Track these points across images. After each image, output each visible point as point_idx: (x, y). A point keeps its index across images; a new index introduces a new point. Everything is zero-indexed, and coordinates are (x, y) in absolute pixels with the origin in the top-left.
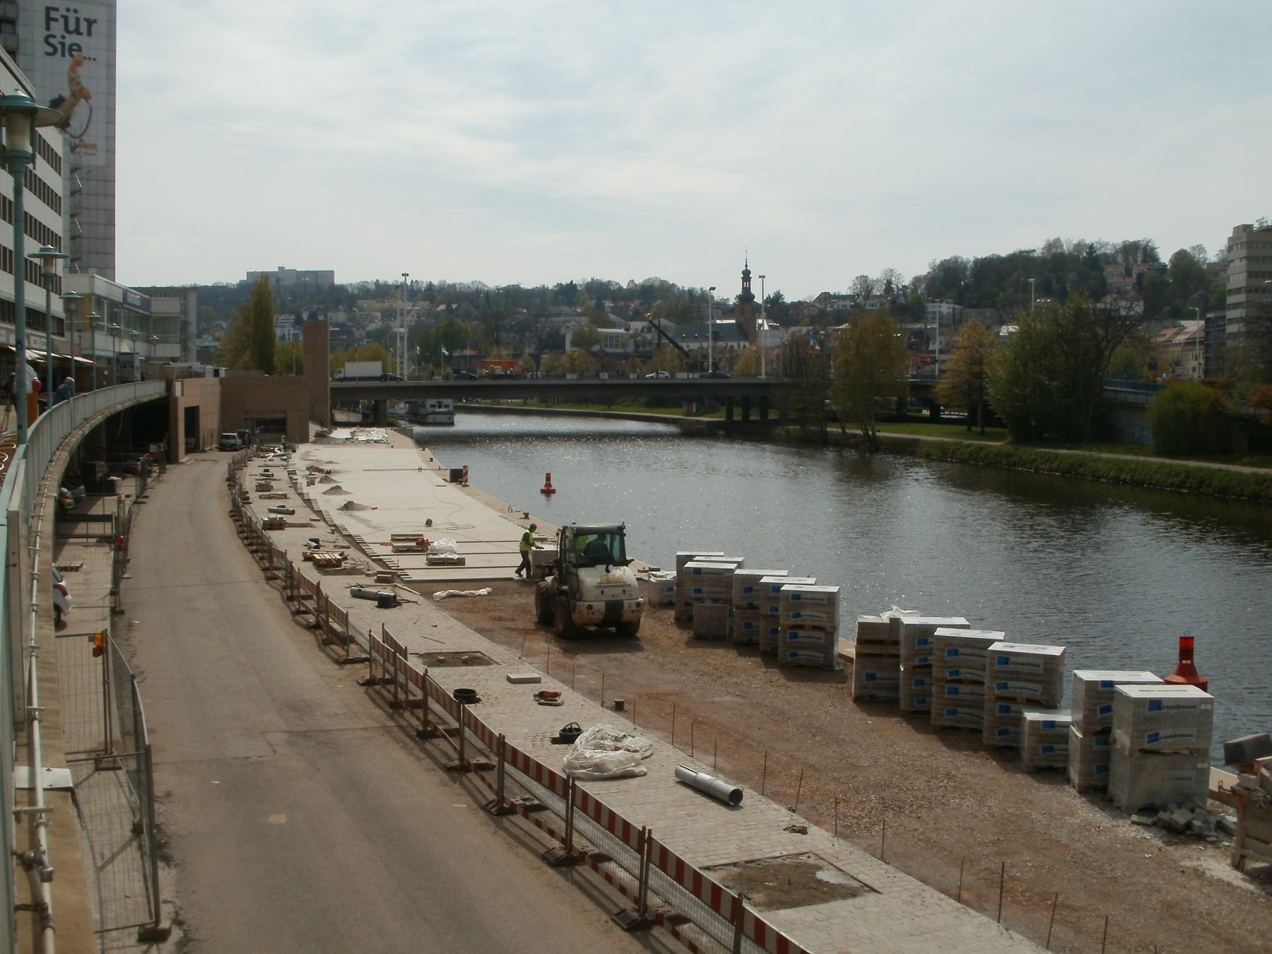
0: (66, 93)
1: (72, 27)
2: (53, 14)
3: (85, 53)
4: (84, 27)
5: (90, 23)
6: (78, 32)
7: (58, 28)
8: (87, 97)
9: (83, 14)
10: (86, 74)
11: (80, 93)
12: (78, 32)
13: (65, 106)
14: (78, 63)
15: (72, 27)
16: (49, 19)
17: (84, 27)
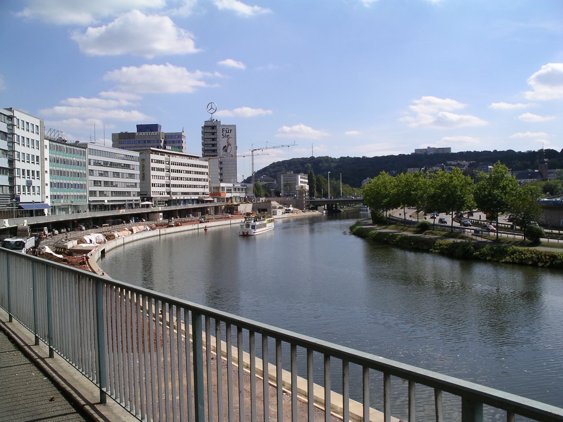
0: (227, 145)
1: (227, 132)
2: (224, 130)
3: (230, 136)
4: (229, 132)
5: (231, 130)
6: (228, 132)
7: (224, 132)
8: (230, 145)
9: (229, 129)
10: (231, 141)
11: (229, 145)
12: (228, 132)
13: (226, 148)
14: (229, 139)
15: (227, 132)
16: (223, 131)
17: (229, 132)
